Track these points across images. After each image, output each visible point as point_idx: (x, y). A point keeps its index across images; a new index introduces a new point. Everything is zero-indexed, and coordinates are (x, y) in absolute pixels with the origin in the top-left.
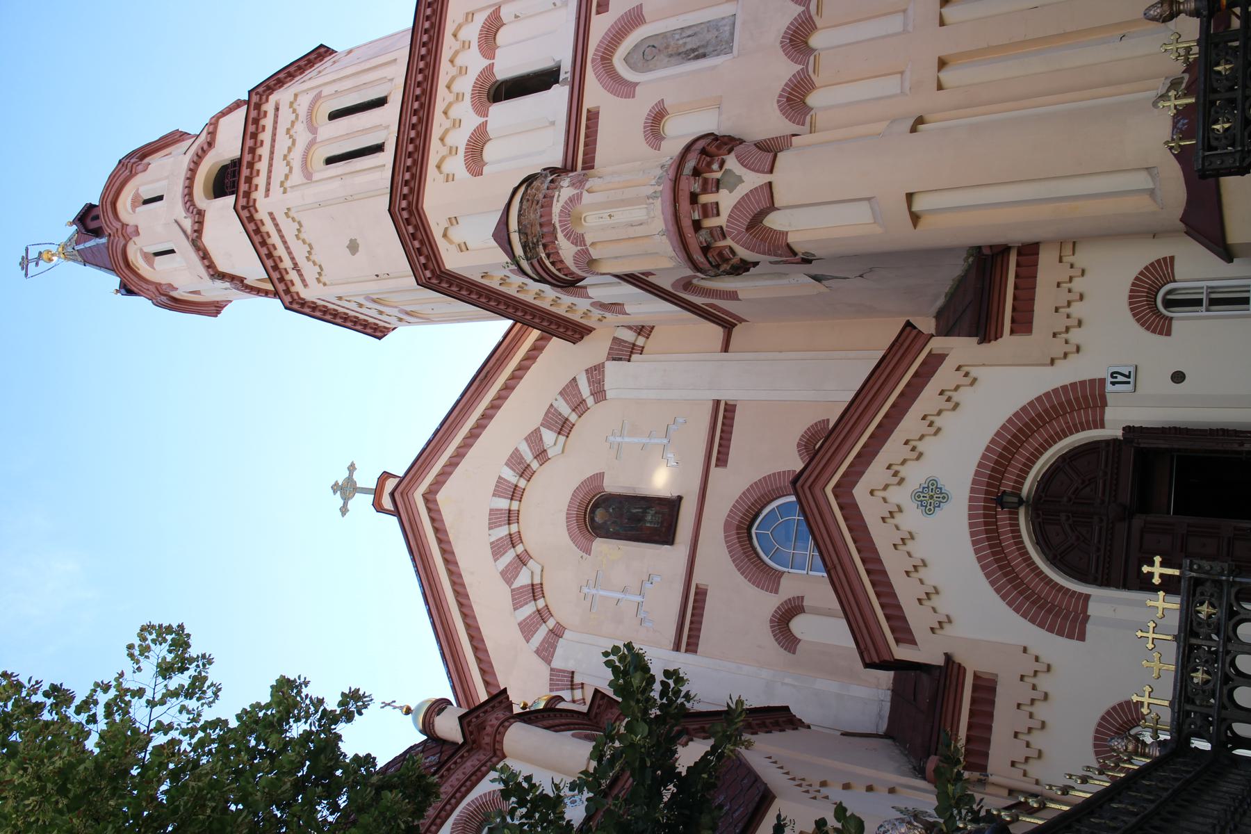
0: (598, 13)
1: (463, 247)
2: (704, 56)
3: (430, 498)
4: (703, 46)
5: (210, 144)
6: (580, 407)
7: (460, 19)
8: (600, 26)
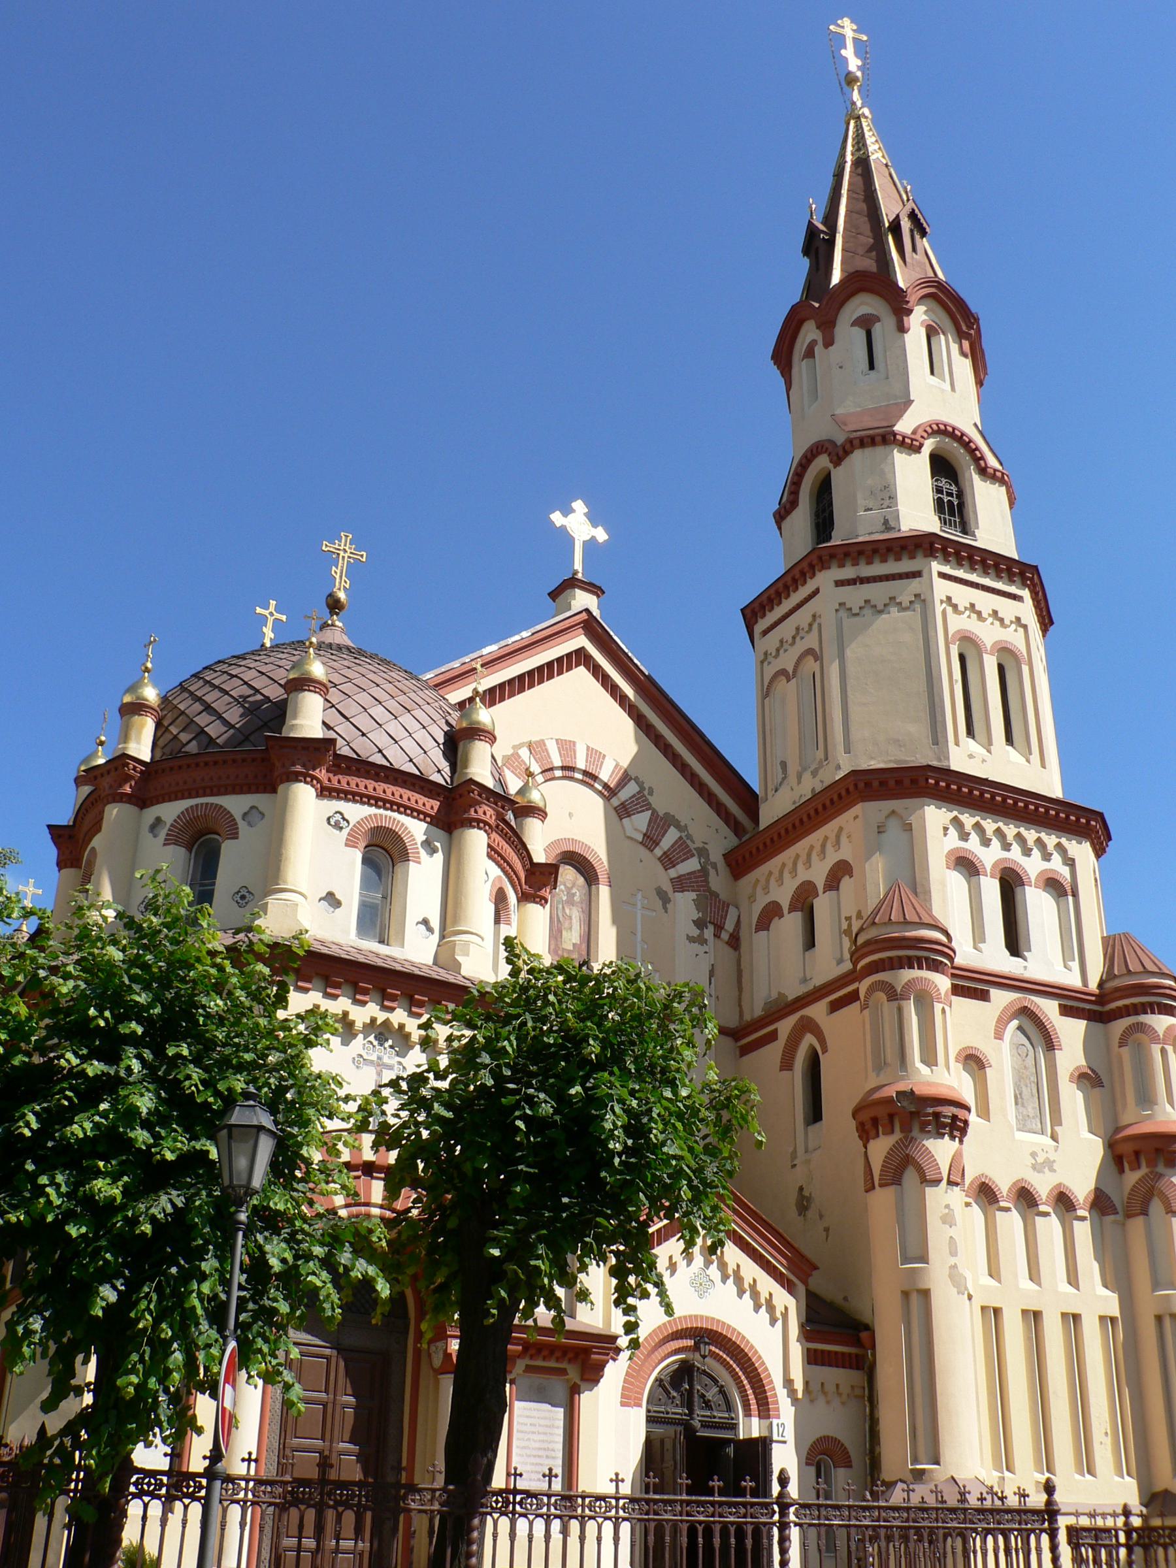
0: (1060, 1005)
1: (881, 830)
2: (1016, 1104)
3: (579, 657)
4: (1023, 1106)
5: (983, 471)
6: (668, 861)
7: (1071, 854)
8: (1049, 1008)
